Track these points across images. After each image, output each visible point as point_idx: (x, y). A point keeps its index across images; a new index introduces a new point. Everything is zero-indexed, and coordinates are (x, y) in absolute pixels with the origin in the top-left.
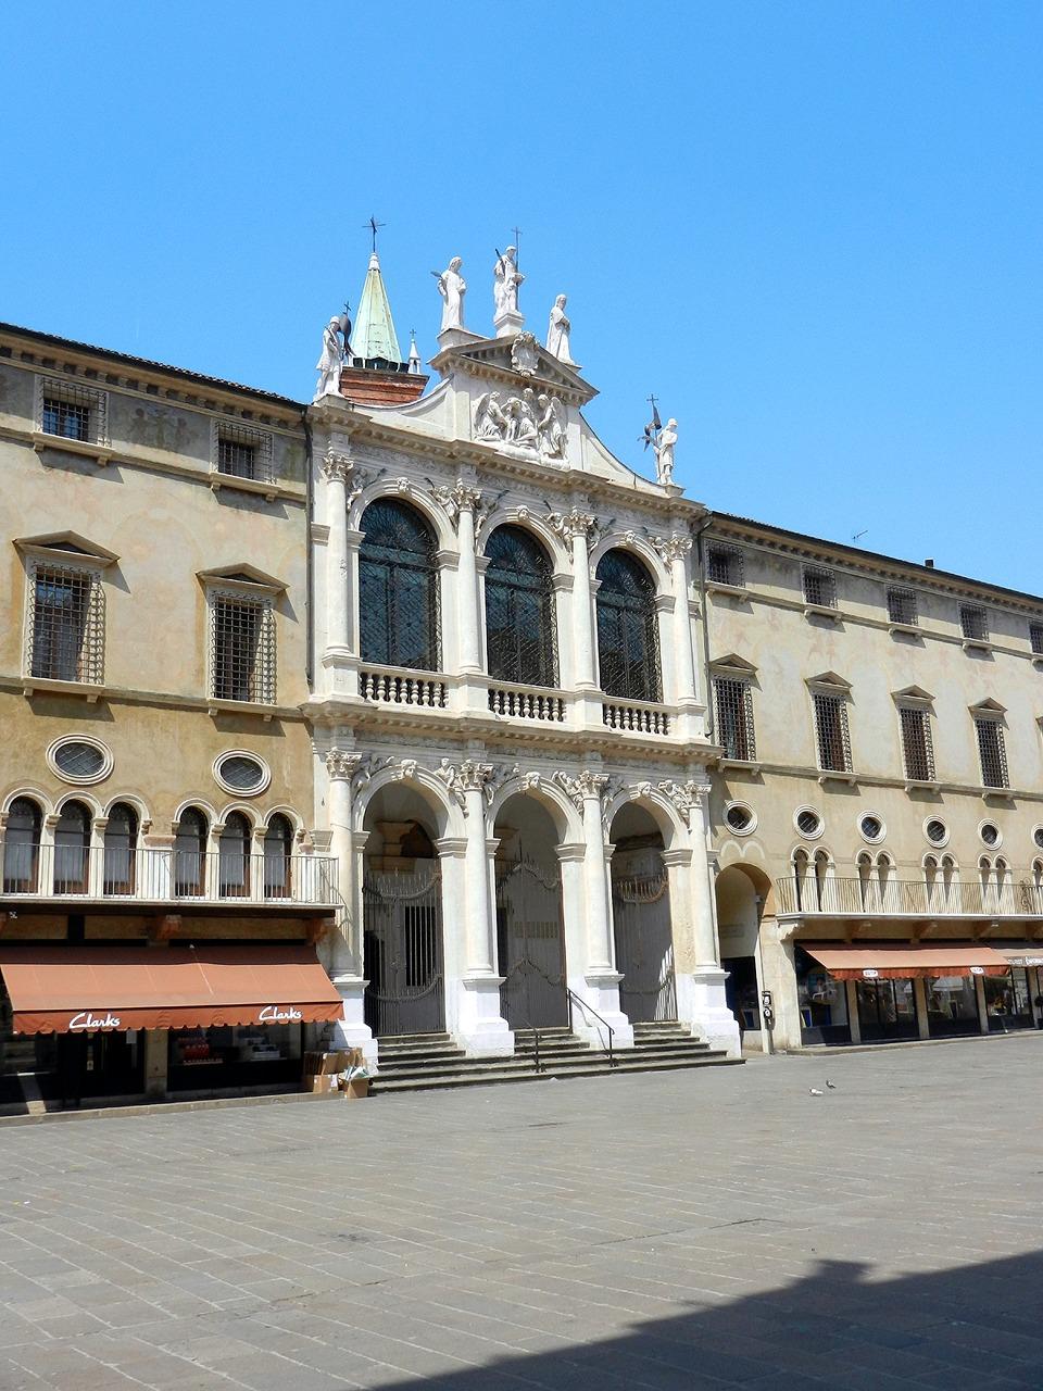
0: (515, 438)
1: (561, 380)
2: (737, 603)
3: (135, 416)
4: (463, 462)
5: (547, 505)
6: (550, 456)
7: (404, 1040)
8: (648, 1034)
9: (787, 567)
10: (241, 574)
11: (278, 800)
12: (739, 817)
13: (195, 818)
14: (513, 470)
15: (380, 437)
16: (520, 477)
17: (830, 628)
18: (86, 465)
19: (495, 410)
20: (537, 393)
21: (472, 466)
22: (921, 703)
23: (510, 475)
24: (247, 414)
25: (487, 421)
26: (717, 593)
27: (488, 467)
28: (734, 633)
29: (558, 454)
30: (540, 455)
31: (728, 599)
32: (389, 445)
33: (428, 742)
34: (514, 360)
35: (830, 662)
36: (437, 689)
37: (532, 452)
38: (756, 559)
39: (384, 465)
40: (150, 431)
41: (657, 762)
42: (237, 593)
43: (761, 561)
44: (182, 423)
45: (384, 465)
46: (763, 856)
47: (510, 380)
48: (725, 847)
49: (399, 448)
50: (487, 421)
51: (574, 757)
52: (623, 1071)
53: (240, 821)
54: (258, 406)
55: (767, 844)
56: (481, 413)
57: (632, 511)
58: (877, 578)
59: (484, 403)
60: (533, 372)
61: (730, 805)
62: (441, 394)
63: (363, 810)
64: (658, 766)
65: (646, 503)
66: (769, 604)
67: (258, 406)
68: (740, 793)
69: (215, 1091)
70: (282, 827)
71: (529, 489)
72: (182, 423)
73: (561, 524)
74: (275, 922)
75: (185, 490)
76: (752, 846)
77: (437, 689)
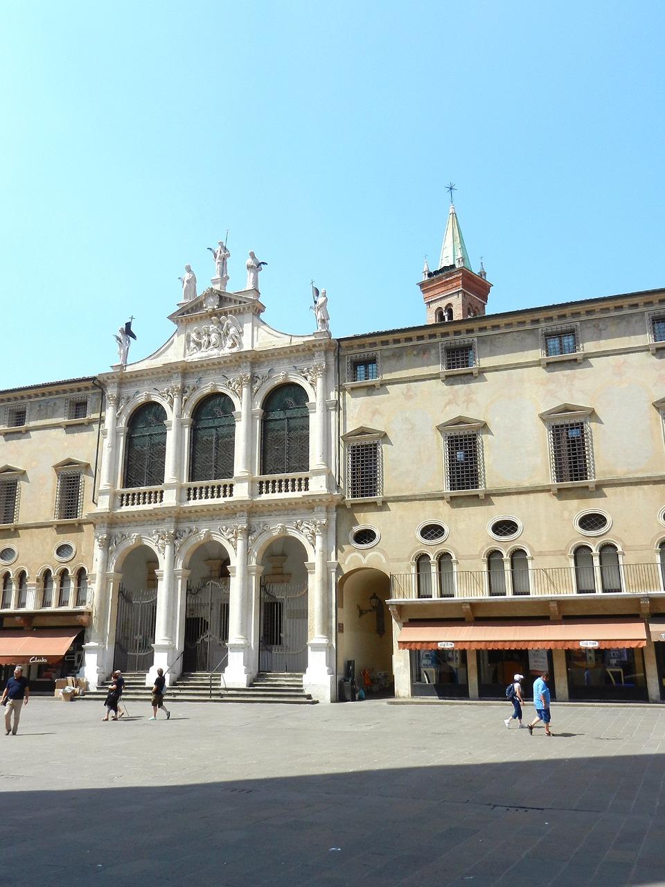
2: (373, 390)
3: (38, 408)
5: (225, 376)
6: (230, 348)
7: (134, 675)
8: (276, 681)
9: (424, 350)
10: (70, 462)
11: (79, 561)
12: (365, 536)
13: (47, 573)
14: (202, 366)
15: (131, 377)
16: (209, 368)
17: (468, 383)
18: (19, 435)
20: (219, 317)
22: (579, 416)
24: (79, 390)
26: (352, 389)
28: (360, 412)
31: (365, 390)
32: (138, 378)
33: (149, 523)
35: (467, 407)
36: (228, 488)
38: (394, 355)
39: (137, 389)
40: (43, 413)
41: (295, 510)
42: (69, 471)
43: (398, 355)
44: (55, 404)
45: (137, 389)
46: (384, 561)
48: (349, 558)
51: (286, 512)
52: (215, 701)
53: (64, 573)
54: (66, 387)
55: (393, 547)
56: (188, 340)
57: (287, 358)
58: (528, 327)
59: (188, 337)
61: (356, 529)
62: (172, 339)
63: (115, 561)
64: (297, 512)
65: (291, 352)
66: (405, 382)
67: (66, 387)
68: (368, 520)
69: (43, 693)
70: (81, 573)
72: (55, 404)
74: (48, 618)
75: (53, 432)
76: (377, 556)
77: (228, 488)
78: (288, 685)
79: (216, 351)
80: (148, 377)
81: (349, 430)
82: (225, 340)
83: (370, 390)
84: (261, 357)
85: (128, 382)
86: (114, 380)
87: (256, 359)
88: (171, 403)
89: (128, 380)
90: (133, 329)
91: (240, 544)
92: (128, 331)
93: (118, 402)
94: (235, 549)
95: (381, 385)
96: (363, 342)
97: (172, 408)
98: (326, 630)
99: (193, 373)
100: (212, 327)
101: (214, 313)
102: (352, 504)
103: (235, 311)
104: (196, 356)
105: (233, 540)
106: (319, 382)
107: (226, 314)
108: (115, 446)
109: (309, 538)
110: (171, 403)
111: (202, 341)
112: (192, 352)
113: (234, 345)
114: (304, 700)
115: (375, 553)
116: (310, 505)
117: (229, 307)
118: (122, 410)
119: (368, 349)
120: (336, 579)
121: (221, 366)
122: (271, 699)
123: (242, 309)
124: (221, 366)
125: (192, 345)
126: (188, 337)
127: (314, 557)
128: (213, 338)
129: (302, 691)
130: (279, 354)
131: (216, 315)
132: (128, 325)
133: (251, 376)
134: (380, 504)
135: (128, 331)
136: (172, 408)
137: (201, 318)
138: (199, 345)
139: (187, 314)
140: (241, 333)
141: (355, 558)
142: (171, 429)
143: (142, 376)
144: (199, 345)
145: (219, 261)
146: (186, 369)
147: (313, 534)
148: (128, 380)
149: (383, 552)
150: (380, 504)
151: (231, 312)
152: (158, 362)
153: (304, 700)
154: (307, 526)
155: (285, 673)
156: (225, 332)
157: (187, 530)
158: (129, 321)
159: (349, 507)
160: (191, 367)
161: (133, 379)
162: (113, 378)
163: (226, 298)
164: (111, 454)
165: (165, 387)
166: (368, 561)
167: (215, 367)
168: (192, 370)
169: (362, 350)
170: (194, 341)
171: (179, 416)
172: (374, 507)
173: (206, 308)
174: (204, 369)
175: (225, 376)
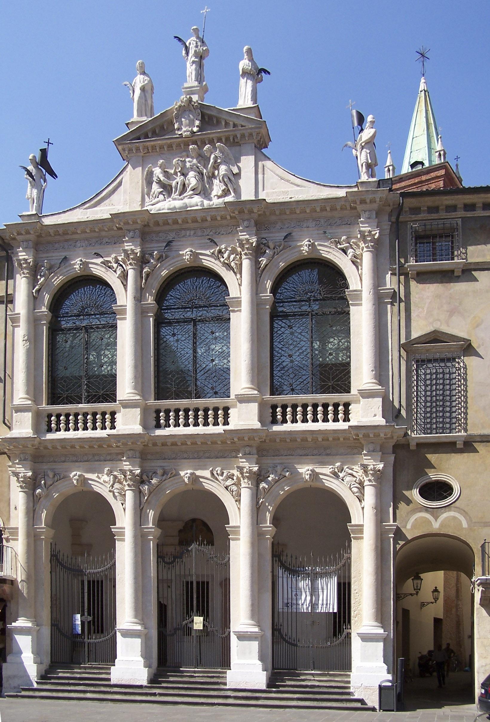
4: (127, 230)
12: (438, 491)
14: (176, 222)
15: (57, 233)
16: (187, 226)
20: (200, 148)
23: (175, 227)
28: (431, 309)
46: (465, 524)
50: (156, 188)
57: (314, 220)
65: (323, 209)
68: (448, 469)
71: (199, 233)
76: (454, 518)
78: (326, 687)
79: (197, 199)
80: (83, 236)
81: (415, 335)
82: (211, 184)
83: (446, 276)
84: (273, 213)
85: (49, 243)
86: (28, 236)
87: (266, 220)
88: (124, 277)
90: (50, 159)
91: (246, 495)
92: (43, 162)
93: (34, 273)
94: (238, 501)
95: (463, 271)
96: (436, 204)
97: (125, 286)
98: (380, 616)
100: (189, 162)
101: (192, 138)
102: (419, 445)
103: (227, 139)
104: (164, 205)
105: (234, 488)
106: (367, 258)
108: (33, 338)
109: (355, 490)
110: (124, 277)
111: (174, 183)
113: (226, 193)
114: (359, 705)
115: (452, 514)
116: (355, 442)
117: (212, 132)
118: (42, 285)
119: (443, 214)
120: (395, 548)
121: (206, 224)
122: (55, 694)
123: (239, 136)
124: (206, 224)
125: (156, 188)
126: (150, 174)
127: (363, 514)
128: (192, 179)
129: (349, 694)
130: (303, 211)
131: (195, 143)
132: (44, 152)
133: (257, 241)
134: (460, 445)
135: (43, 162)
136: (125, 286)
138: (167, 189)
139: (147, 140)
140: (238, 175)
141: (419, 519)
142: (125, 319)
144: (167, 189)
145: (193, 59)
146: (146, 225)
147: (361, 483)
149: (465, 513)
150: (460, 445)
151: (220, 140)
152: (102, 212)
153: (359, 705)
154: (350, 471)
155: (313, 672)
157: (160, 472)
159: (413, 447)
160: (157, 224)
161: (58, 237)
162: (28, 233)
163: (211, 117)
164: (28, 352)
166: (441, 525)
167: (195, 225)
169: (434, 216)
170: (159, 182)
171: (139, 298)
172: (450, 447)
173: (179, 129)
175: (212, 241)
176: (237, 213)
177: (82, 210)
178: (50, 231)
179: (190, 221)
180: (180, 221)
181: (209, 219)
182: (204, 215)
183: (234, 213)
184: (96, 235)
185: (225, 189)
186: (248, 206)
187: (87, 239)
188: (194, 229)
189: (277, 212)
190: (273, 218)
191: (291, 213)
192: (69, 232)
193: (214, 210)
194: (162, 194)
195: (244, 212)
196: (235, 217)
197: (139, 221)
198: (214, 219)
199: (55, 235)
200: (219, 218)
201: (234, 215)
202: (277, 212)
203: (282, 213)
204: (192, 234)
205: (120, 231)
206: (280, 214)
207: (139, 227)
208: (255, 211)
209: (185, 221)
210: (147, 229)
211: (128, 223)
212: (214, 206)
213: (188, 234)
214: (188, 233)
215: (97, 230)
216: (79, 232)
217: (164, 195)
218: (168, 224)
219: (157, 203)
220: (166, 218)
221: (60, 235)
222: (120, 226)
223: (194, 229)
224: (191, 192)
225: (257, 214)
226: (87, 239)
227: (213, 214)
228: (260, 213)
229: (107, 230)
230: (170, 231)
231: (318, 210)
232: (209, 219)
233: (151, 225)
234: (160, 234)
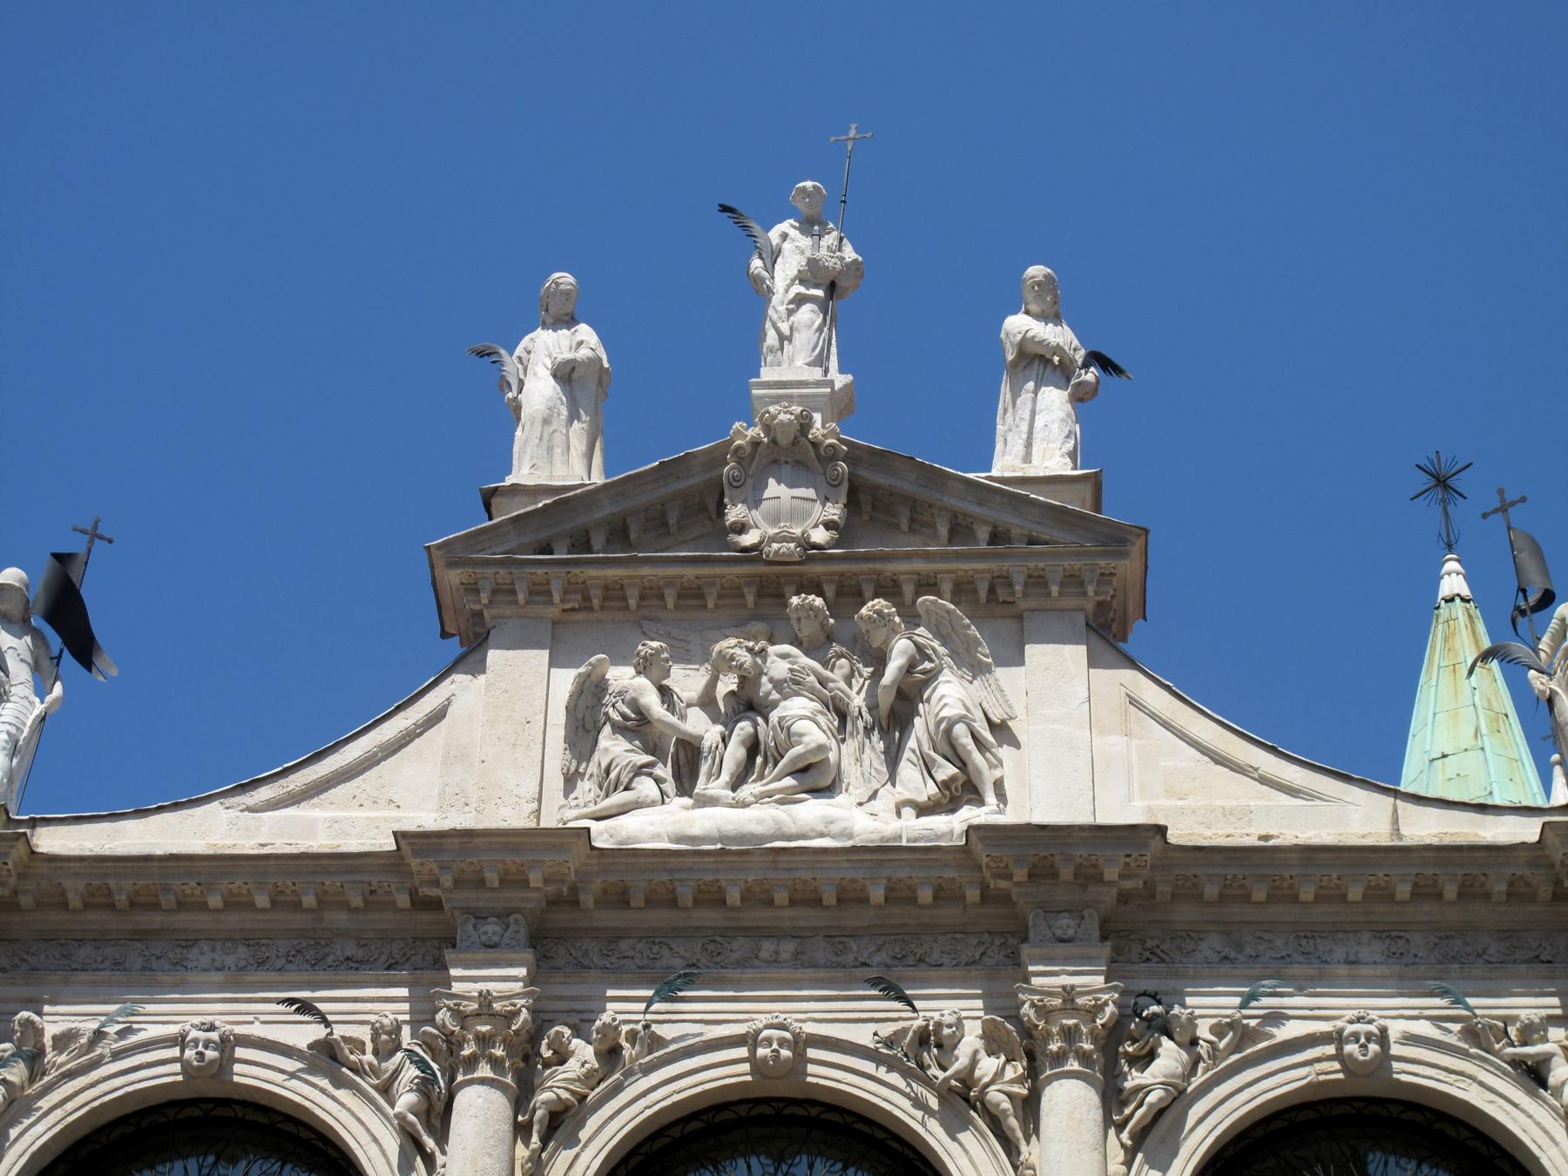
0: (736, 784)
1: (983, 533)
4: (467, 911)
6: (923, 810)
14: (712, 898)
16: (759, 916)
19: (635, 705)
21: (503, 915)
23: (708, 917)
25: (614, 748)
27: (582, 918)
29: (962, 790)
30: (872, 808)
32: (155, 920)
34: (735, 513)
37: (811, 811)
47: (731, 593)
49: (200, 921)
50: (614, 748)
60: (820, 536)
65: (1426, 892)
73: (971, 1039)
80: (233, 920)
84: (1189, 892)
89: (55, 918)
99: (613, 937)
104: (657, 822)
107: (888, 589)
112: (620, 797)
121: (854, 918)
137: (692, 595)
143: (182, 905)
146: (571, 901)
148: (55, 918)
156: (886, 700)
158: (73, 544)
161: (97, 919)
165: (368, 1008)
167: (807, 917)
168: (610, 919)
174: (708, 917)
176: (1020, 874)
177: (233, 813)
178: (68, 883)
179: (781, 897)
180: (734, 896)
181: (877, 894)
182: (859, 875)
183: (1009, 877)
184: (299, 921)
185: (953, 779)
186: (1080, 853)
187: (249, 939)
188: (796, 935)
189: (1211, 891)
190: (1185, 913)
191: (1272, 899)
192: (167, 900)
193: (906, 856)
194: (650, 775)
195: (1055, 875)
196: (1005, 899)
197: (535, 879)
198: (900, 895)
199: (87, 906)
200: (925, 895)
201: (1003, 884)
202: (1211, 891)
203: (1235, 895)
204: (784, 956)
205: (426, 917)
206: (1222, 899)
207: (532, 900)
208: (1111, 873)
209: (759, 897)
210: (562, 918)
211: (480, 883)
212: (904, 843)
213: (764, 954)
214: (767, 948)
215: (309, 900)
216: (215, 901)
217: (658, 781)
218: (673, 902)
219: (623, 810)
220: (665, 878)
221: (112, 906)
222: (434, 892)
223: (796, 935)
224: (789, 781)
225: (1114, 891)
226: (249, 939)
227: (903, 874)
228: (1128, 884)
229: (357, 901)
230: (677, 933)
231: (1404, 891)
232: (877, 894)
233: (587, 900)
234: (624, 945)
